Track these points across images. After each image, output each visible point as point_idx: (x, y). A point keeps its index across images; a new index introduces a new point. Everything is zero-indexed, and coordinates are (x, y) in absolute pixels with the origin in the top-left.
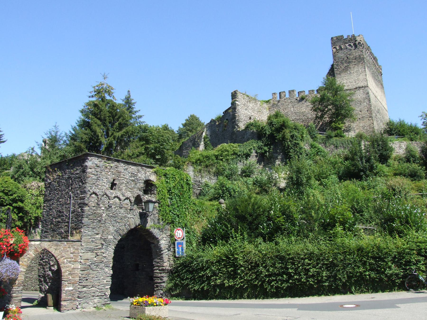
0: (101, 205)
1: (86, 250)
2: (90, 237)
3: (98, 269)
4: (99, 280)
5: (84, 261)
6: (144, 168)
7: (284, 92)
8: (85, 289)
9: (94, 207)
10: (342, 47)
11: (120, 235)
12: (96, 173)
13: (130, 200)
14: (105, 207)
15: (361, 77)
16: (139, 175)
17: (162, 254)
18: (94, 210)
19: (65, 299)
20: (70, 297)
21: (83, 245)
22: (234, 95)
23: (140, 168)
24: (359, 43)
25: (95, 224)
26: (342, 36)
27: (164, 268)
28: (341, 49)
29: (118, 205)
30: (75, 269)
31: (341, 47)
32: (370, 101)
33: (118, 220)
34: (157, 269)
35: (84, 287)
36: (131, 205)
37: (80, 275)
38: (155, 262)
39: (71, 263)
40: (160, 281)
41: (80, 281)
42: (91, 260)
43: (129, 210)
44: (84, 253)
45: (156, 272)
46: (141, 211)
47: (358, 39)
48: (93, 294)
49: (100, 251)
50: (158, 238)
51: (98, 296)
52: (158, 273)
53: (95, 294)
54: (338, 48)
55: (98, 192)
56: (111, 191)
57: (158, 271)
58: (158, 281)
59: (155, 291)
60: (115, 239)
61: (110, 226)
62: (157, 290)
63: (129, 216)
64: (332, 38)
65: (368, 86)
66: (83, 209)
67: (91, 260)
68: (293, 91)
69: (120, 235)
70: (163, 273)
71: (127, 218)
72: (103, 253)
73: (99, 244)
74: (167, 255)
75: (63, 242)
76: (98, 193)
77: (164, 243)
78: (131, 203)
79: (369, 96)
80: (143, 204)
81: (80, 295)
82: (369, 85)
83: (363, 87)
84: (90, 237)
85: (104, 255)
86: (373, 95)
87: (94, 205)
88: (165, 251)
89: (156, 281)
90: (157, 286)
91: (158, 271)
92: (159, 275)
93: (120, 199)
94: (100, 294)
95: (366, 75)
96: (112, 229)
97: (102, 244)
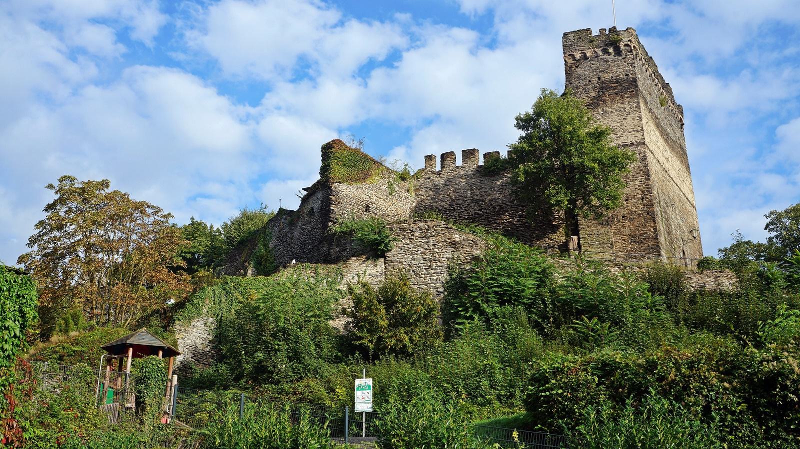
7: (452, 153)
10: (588, 55)
15: (629, 122)
26: (588, 30)
28: (585, 57)
31: (585, 55)
54: (578, 55)
64: (565, 34)
65: (644, 143)
79: (646, 166)
82: (647, 141)
83: (632, 144)
86: (659, 166)
95: (641, 119)
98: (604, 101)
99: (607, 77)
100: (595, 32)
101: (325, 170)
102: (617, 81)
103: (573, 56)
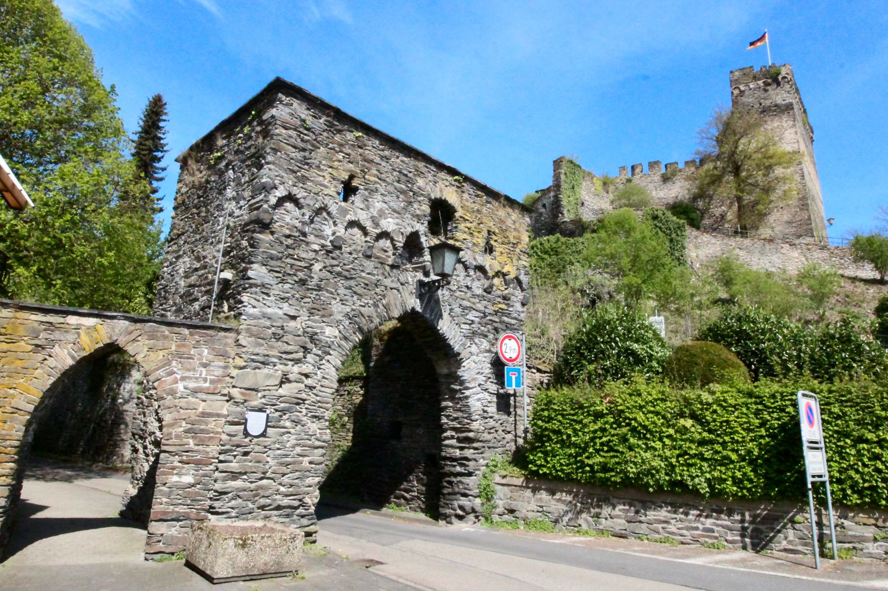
0: (311, 238)
1: (253, 360)
2: (268, 323)
3: (288, 424)
4: (286, 456)
5: (243, 394)
6: (432, 168)
8: (238, 483)
9: (288, 236)
11: (360, 330)
12: (301, 145)
13: (392, 240)
14: (323, 246)
16: (421, 182)
17: (467, 397)
18: (288, 247)
19: (165, 513)
20: (182, 509)
21: (243, 342)
22: (557, 164)
23: (421, 165)
24: (784, 78)
25: (287, 286)
26: (751, 67)
27: (471, 435)
29: (359, 248)
30: (210, 415)
32: (803, 176)
33: (358, 290)
34: (452, 437)
35: (235, 476)
36: (394, 254)
37: (224, 437)
38: (448, 417)
39: (199, 395)
40: (458, 469)
41: (222, 457)
42: (266, 393)
43: (387, 268)
44: (241, 368)
45: (447, 446)
46: (420, 276)
47: (784, 71)
48: (263, 501)
49: (296, 369)
50: (459, 354)
51: (278, 508)
52: (452, 447)
53: (268, 501)
55: (304, 198)
56: (343, 204)
57: (453, 442)
58: (452, 469)
59: (444, 495)
60: (346, 338)
61: (333, 302)
62: (449, 494)
63: (388, 282)
66: (252, 238)
67: (266, 393)
68: (657, 163)
69: (360, 330)
70: (469, 448)
71: (383, 288)
72: (307, 376)
73: (296, 348)
74: (479, 400)
75: (176, 329)
76: (302, 201)
77: (474, 368)
78: (395, 248)
79: (801, 169)
80: (427, 257)
81: (216, 504)
84: (268, 323)
85: (309, 382)
87: (288, 232)
88: (474, 390)
89: (447, 469)
90: (450, 483)
91: (453, 442)
92: (458, 453)
93: (365, 233)
94: (286, 501)
96: (338, 309)
97: (305, 349)
98: (766, 122)
99: (768, 103)
100: (757, 69)
101: (557, 177)
102: (776, 106)
103: (739, 88)
